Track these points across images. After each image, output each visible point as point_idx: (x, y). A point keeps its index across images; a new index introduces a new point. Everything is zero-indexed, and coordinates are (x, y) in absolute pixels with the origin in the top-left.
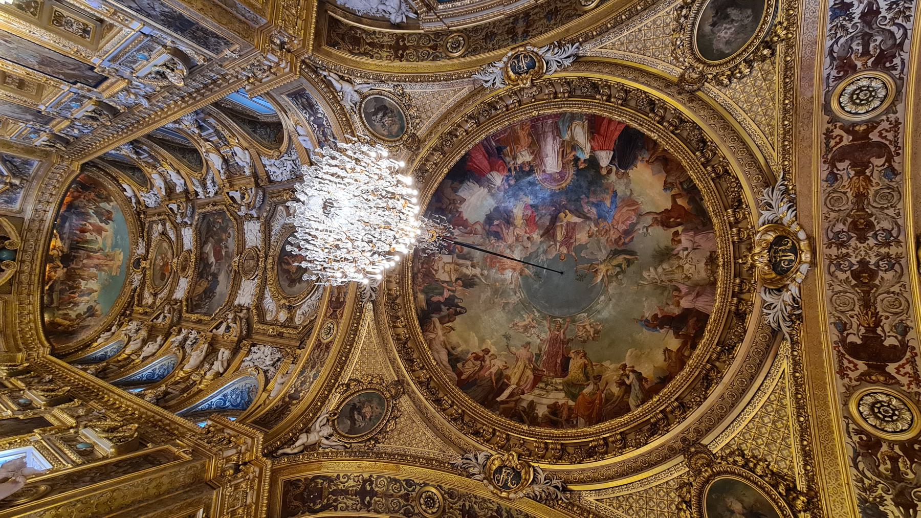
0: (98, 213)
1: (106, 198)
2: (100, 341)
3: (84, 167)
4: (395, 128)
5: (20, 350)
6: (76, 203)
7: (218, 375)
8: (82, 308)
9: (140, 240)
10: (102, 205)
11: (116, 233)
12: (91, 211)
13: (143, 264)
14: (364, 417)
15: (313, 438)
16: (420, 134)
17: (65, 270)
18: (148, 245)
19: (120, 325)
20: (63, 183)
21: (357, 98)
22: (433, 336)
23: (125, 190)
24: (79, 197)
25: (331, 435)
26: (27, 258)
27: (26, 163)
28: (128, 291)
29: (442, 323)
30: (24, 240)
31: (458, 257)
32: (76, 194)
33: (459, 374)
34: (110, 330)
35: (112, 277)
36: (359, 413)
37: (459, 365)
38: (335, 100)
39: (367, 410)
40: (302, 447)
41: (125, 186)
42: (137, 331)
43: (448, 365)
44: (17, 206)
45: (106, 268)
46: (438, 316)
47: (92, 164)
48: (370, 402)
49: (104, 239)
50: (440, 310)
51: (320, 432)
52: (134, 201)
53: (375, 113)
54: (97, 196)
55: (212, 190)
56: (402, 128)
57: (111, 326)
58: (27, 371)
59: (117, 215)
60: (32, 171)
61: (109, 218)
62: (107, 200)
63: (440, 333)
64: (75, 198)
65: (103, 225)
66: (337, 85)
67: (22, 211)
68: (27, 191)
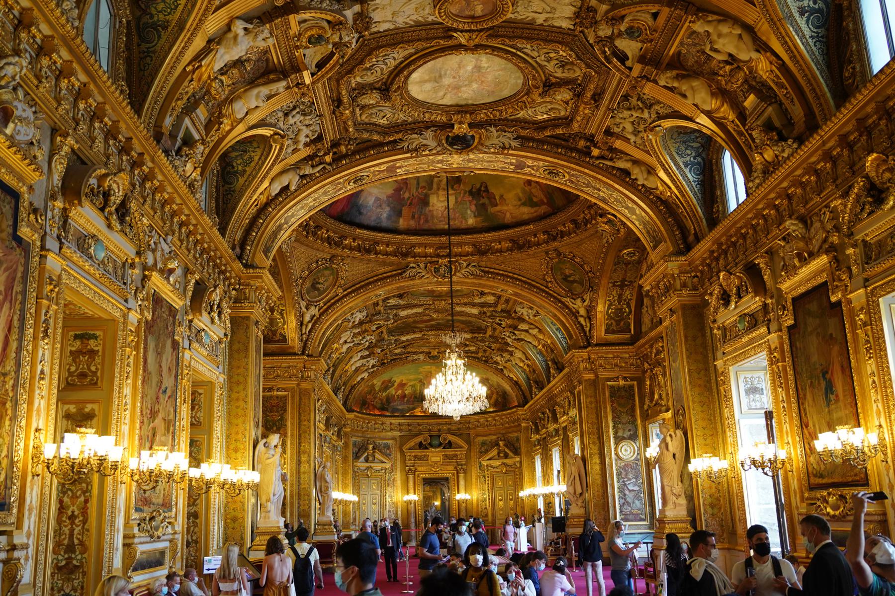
2: (511, 375)
3: (350, 410)
4: (327, 272)
5: (520, 425)
7: (540, 331)
12: (384, 394)
14: (572, 274)
15: (582, 312)
16: (328, 256)
18: (414, 353)
19: (497, 363)
21: (313, 308)
22: (508, 215)
26: (436, 428)
27: (355, 445)
29: (496, 205)
31: (431, 188)
32: (371, 408)
33: (541, 203)
36: (570, 276)
37: (535, 200)
39: (567, 272)
41: (359, 379)
43: (535, 209)
44: (390, 442)
46: (489, 207)
48: (561, 269)
49: (410, 380)
50: (483, 204)
51: (579, 306)
53: (318, 289)
55: (368, 338)
56: (326, 268)
57: (497, 369)
58: (536, 425)
59: (385, 377)
60: (359, 439)
62: (373, 386)
63: (505, 208)
64: (375, 407)
65: (396, 384)
66: (310, 325)
67: (394, 438)
68: (376, 438)
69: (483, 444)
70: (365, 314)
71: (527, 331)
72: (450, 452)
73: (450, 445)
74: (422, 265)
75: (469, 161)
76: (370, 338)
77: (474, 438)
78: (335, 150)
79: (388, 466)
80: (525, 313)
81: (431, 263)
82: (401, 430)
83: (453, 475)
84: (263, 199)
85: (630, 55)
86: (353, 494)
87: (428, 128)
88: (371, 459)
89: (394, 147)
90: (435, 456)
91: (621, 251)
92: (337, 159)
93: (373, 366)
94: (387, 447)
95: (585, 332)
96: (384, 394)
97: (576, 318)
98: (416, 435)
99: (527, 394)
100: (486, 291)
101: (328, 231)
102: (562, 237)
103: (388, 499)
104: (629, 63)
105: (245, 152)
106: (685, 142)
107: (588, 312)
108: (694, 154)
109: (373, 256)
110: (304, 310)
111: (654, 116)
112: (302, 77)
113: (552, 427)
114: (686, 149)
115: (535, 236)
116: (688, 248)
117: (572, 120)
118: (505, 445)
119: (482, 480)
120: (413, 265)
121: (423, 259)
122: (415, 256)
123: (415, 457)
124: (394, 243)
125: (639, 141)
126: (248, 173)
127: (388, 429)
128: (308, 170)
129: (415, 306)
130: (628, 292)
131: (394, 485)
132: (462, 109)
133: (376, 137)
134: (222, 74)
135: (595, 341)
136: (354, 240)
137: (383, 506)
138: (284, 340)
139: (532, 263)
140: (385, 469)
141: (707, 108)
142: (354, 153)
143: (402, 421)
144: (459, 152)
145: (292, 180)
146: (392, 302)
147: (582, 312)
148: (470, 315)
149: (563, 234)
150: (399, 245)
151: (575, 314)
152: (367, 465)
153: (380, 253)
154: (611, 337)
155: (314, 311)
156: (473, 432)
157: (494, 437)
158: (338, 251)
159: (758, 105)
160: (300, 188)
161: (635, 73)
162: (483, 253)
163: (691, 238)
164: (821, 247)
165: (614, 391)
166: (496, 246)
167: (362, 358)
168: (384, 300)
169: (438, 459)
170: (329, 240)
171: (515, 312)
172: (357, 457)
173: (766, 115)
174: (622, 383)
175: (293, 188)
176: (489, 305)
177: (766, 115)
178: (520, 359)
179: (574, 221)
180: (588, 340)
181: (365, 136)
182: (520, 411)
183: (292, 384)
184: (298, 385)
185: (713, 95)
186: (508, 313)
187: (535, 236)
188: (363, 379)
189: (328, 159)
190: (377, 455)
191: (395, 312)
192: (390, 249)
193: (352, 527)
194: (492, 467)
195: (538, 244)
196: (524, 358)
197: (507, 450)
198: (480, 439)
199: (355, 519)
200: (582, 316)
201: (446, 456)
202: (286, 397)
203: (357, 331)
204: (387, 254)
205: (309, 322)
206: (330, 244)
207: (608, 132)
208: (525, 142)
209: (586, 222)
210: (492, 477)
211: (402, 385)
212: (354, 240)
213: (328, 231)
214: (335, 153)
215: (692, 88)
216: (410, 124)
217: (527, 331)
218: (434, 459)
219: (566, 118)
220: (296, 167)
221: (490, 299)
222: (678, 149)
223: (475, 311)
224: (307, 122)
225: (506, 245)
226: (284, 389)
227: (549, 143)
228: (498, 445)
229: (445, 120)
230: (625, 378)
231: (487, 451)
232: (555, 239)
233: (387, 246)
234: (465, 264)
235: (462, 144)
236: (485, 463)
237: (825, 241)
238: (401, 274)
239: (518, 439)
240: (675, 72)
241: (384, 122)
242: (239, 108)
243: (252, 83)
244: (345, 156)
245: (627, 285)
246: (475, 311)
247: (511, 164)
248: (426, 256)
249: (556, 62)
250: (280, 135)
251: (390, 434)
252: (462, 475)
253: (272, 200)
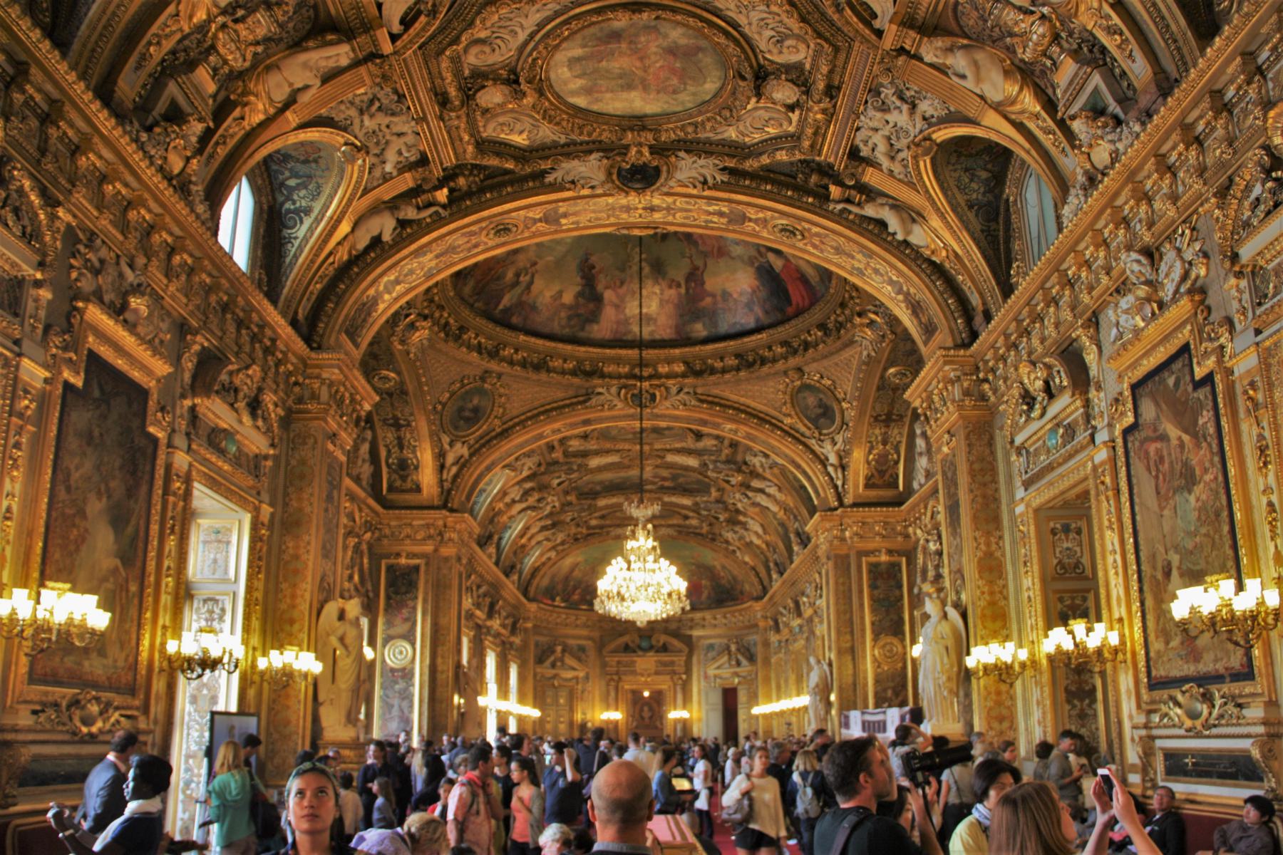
2: (747, 559)
15: (833, 459)
19: (727, 542)
21: (459, 445)
25: (833, 439)
27: (537, 645)
34: (734, 551)
38: (463, 464)
40: (839, 471)
42: (735, 532)
47: (525, 593)
66: (454, 470)
68: (567, 636)
69: (711, 647)
70: (536, 459)
71: (762, 491)
72: (665, 658)
73: (664, 649)
74: (614, 390)
75: (652, 209)
76: (553, 501)
78: (452, 184)
79: (581, 674)
80: (758, 465)
81: (625, 387)
84: (343, 255)
85: (878, 11)
86: (535, 706)
87: (591, 152)
88: (559, 664)
89: (536, 182)
90: (645, 662)
91: (885, 369)
92: (454, 198)
93: (563, 543)
94: (582, 649)
95: (836, 487)
97: (825, 466)
98: (621, 635)
99: (766, 582)
100: (705, 430)
101: (477, 335)
102: (806, 350)
104: (877, 24)
105: (310, 177)
106: (966, 170)
107: (840, 458)
108: (982, 190)
109: (543, 376)
110: (447, 447)
111: (920, 124)
112: (375, 42)
113: (796, 623)
114: (972, 180)
115: (770, 348)
116: (974, 335)
117: (799, 138)
118: (738, 650)
120: (600, 390)
121: (615, 382)
122: (603, 376)
124: (573, 357)
125: (897, 168)
126: (316, 211)
128: (410, 213)
129: (608, 452)
130: (896, 431)
132: (638, 122)
133: (510, 165)
134: (236, 21)
135: (848, 500)
136: (517, 351)
138: (418, 489)
139: (766, 392)
140: (577, 678)
141: (995, 96)
142: (482, 190)
144: (640, 191)
145: (385, 226)
146: (575, 445)
147: (833, 459)
148: (687, 468)
149: (807, 346)
150: (580, 361)
151: (823, 462)
152: (554, 672)
153: (554, 370)
154: (873, 494)
155: (461, 450)
156: (696, 633)
157: (725, 641)
158: (494, 366)
159: (1076, 75)
160: (400, 242)
161: (888, 43)
162: (698, 374)
163: (979, 319)
164: (1177, 291)
165: (874, 569)
166: (718, 365)
167: (544, 528)
168: (562, 441)
170: (479, 349)
171: (746, 463)
172: (540, 661)
173: (1089, 89)
174: (884, 558)
175: (387, 237)
176: (710, 452)
177: (1089, 89)
178: (756, 533)
179: (822, 326)
180: (840, 498)
181: (493, 162)
182: (757, 606)
183: (429, 548)
184: (436, 550)
185: (1007, 74)
186: (739, 465)
187: (770, 348)
188: (549, 559)
189: (442, 195)
190: (569, 661)
191: (579, 461)
192: (570, 365)
195: (774, 361)
196: (760, 531)
197: (740, 657)
200: (832, 465)
202: (417, 568)
203: (528, 485)
204: (563, 373)
205: (453, 464)
206: (480, 353)
207: (854, 154)
208: (737, 178)
209: (840, 326)
212: (517, 351)
213: (477, 335)
214: (451, 191)
215: (976, 64)
216: (563, 146)
217: (762, 491)
219: (792, 136)
220: (392, 205)
221: (708, 443)
222: (959, 180)
223: (693, 462)
224: (396, 129)
225: (732, 362)
226: (415, 556)
227: (773, 182)
228: (728, 648)
229: (614, 138)
230: (890, 552)
232: (795, 352)
233: (565, 361)
234: (674, 390)
235: (641, 177)
236: (711, 672)
237: (1185, 277)
238: (585, 402)
239: (755, 644)
240: (948, 41)
241: (520, 140)
242: (276, 87)
243: (297, 45)
244: (469, 194)
245: (894, 421)
246: (693, 462)
247: (721, 214)
248: (619, 377)
249: (773, 33)
250: (353, 144)
253: (358, 257)
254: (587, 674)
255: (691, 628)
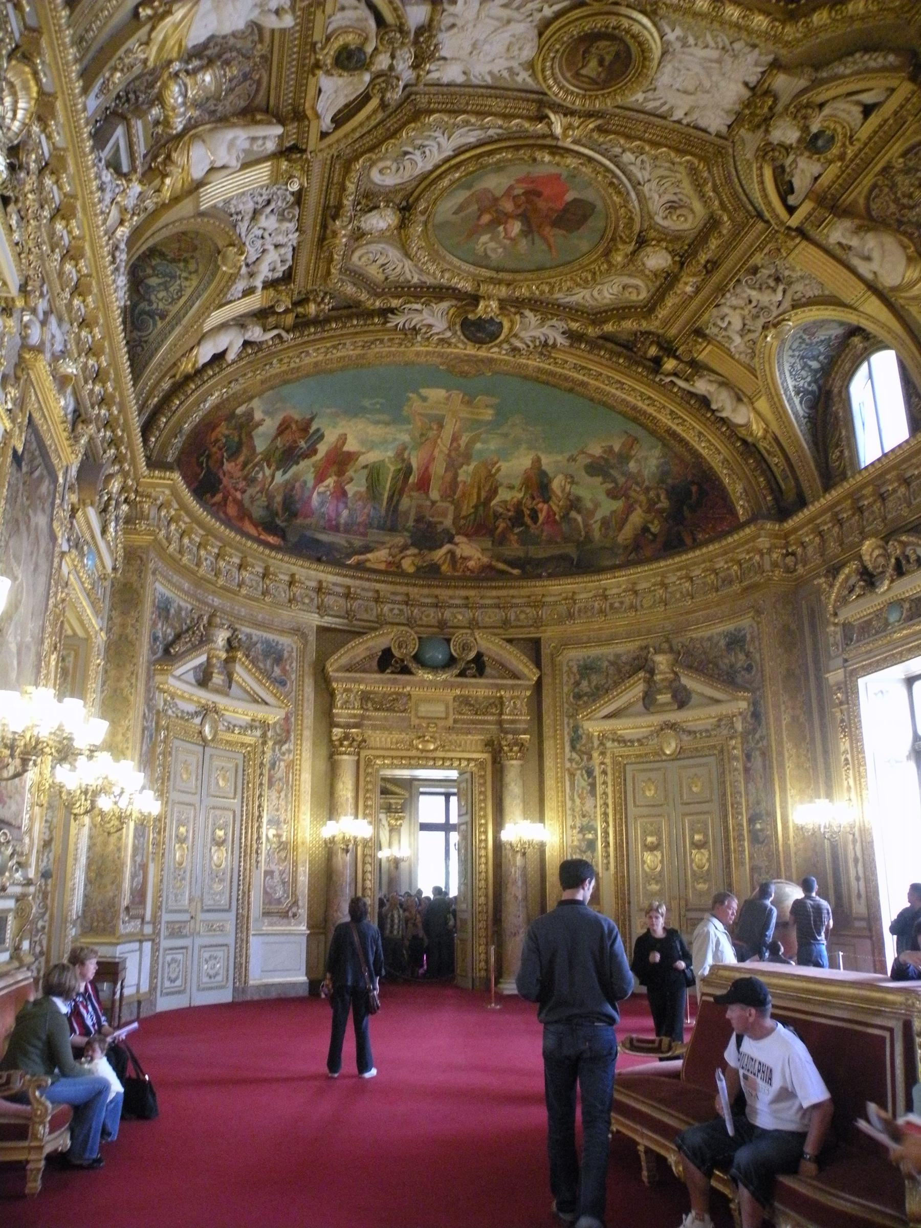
0: (289, 457)
1: (240, 427)
6: (257, 512)
8: (592, 491)
9: (398, 320)
10: (261, 445)
11: (354, 411)
12: (280, 478)
13: (488, 308)
17: (458, 539)
20: (209, 532)
23: (219, 357)
24: (239, 504)
28: (571, 364)
30: (379, 623)
32: (232, 510)
35: (501, 415)
41: (205, 353)
44: (286, 641)
45: (464, 440)
52: (256, 333)
54: (234, 454)
60: (186, 604)
61: (305, 428)
65: (322, 449)
67: (298, 631)
69: (587, 669)
72: (480, 689)
73: (479, 665)
77: (557, 651)
79: (274, 716)
82: (321, 609)
83: (481, 765)
88: (218, 679)
94: (275, 655)
96: (280, 478)
103: (268, 832)
119: (582, 782)
123: (365, 697)
127: (283, 597)
131: (290, 788)
137: (247, 851)
143: (330, 577)
152: (205, 696)
156: (549, 635)
157: (625, 649)
169: (438, 710)
193: (127, 927)
194: (622, 741)
198: (574, 655)
199: (139, 895)
201: (464, 701)
210: (620, 769)
211: (340, 461)
218: (424, 709)
231: (597, 693)
236: (593, 727)
251: (288, 615)
252: (513, 767)
254: (287, 719)
255: (538, 623)
